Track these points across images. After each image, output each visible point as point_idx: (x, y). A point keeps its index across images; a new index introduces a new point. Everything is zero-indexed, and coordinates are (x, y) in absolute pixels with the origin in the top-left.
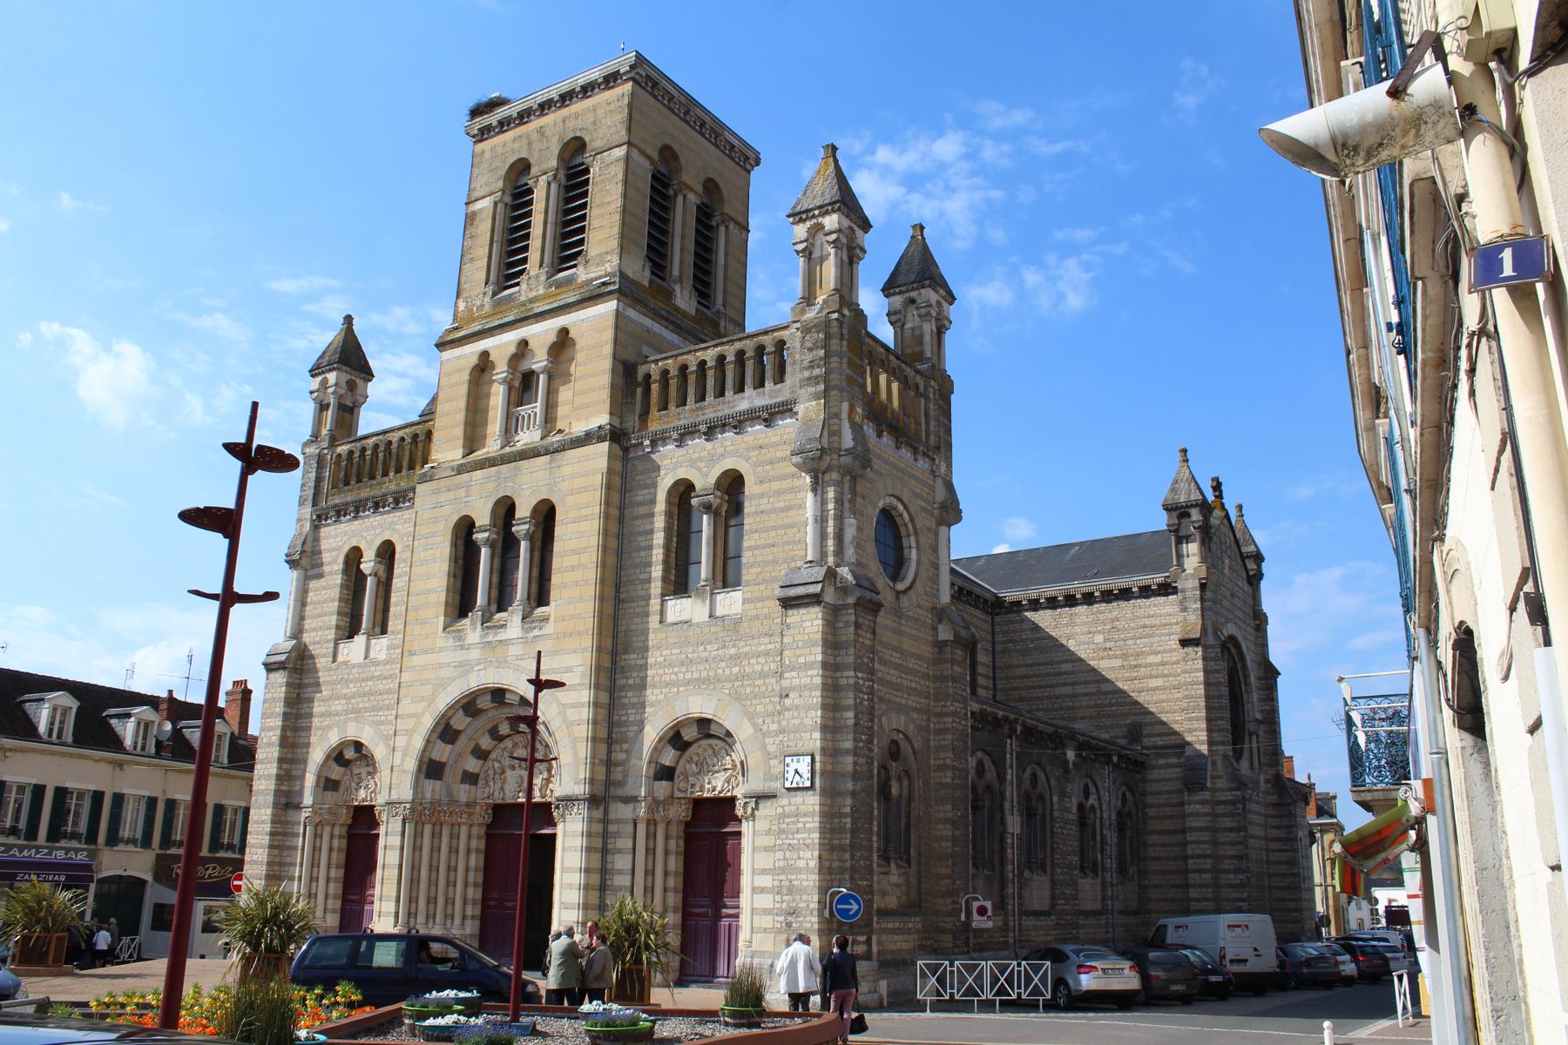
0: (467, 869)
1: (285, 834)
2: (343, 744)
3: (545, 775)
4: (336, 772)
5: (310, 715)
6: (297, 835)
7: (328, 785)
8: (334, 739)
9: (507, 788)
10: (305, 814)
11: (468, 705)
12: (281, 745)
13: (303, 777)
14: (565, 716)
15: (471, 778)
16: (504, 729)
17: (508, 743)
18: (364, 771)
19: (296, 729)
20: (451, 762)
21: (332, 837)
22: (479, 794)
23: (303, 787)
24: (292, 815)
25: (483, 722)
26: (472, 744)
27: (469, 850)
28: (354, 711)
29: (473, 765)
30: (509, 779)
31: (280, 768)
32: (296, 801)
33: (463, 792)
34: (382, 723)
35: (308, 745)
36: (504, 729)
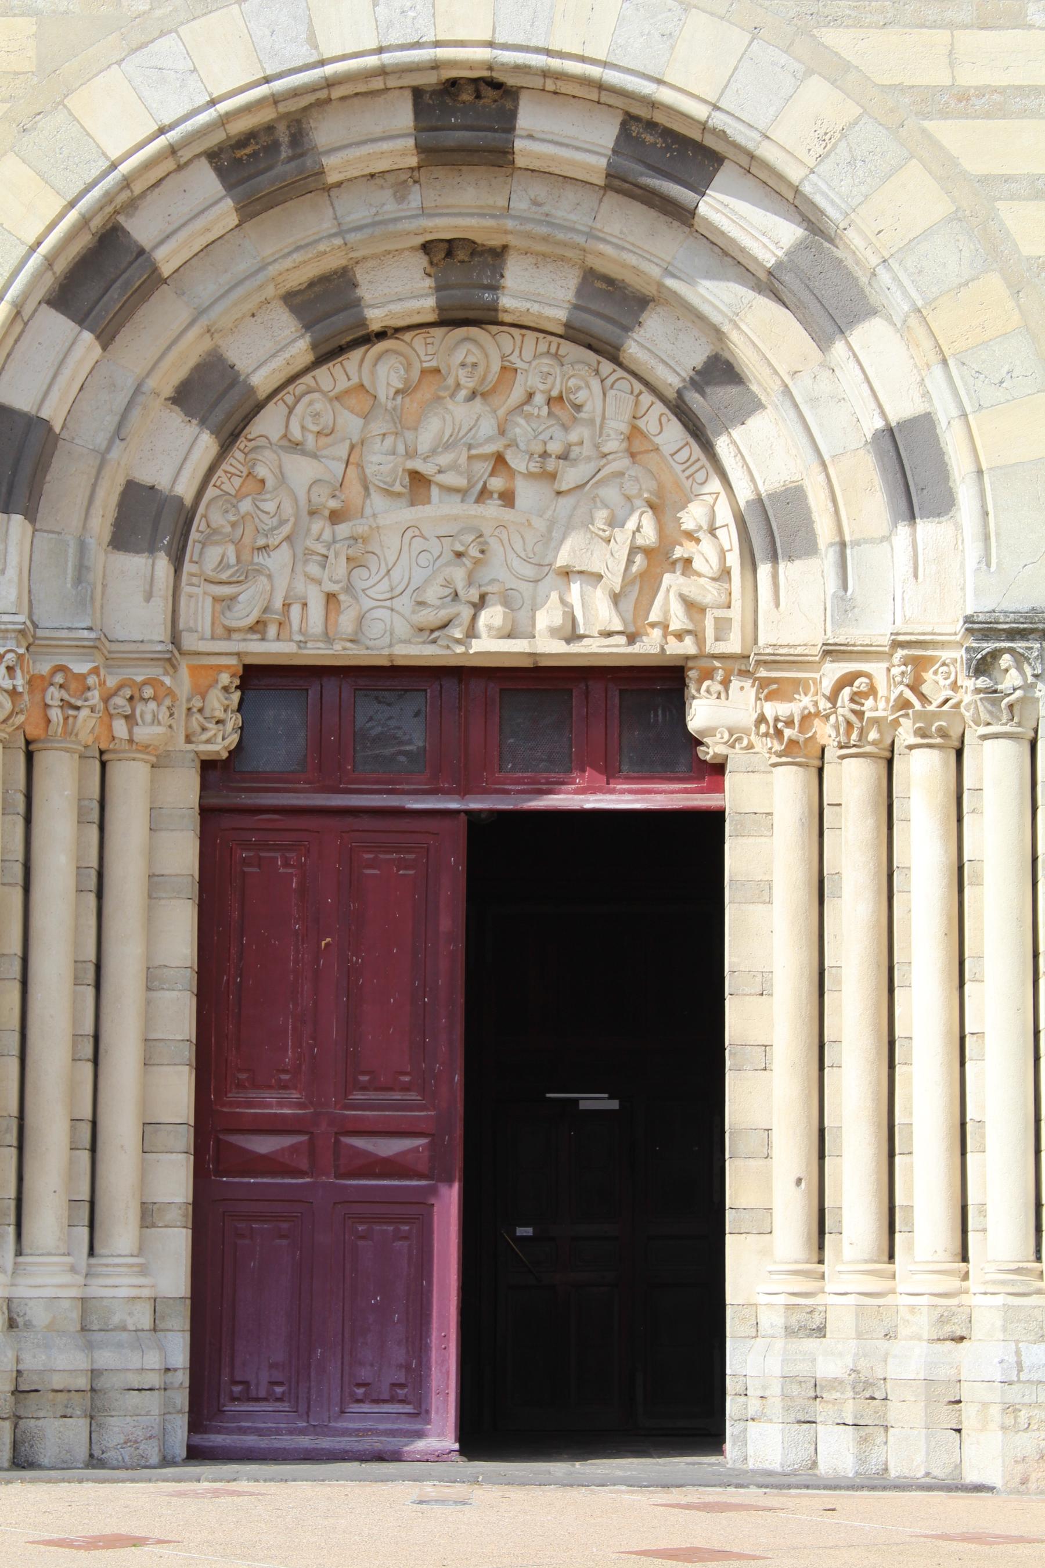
0: (153, 980)
3: (649, 535)
9: (373, 584)
11: (261, 157)
14: (993, 249)
15: (152, 521)
16: (397, 292)
17: (383, 371)
20: (92, 431)
22: (199, 612)
25: (299, 244)
26: (207, 344)
27: (154, 882)
29: (175, 455)
30: (390, 544)
33: (135, 594)
36: (397, 292)
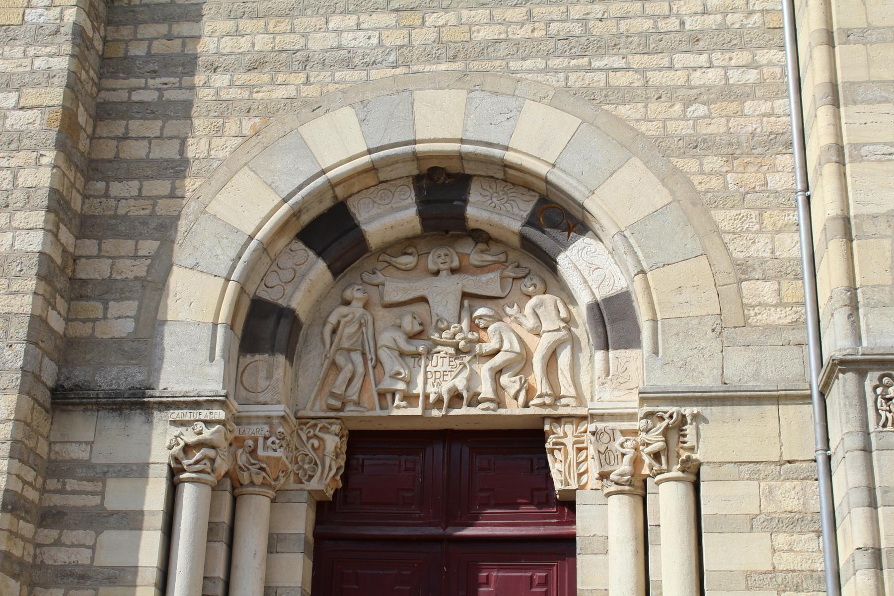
1: (49, 517)
2: (373, 176)
4: (307, 282)
5: (187, 64)
6: (132, 520)
7: (262, 327)
8: (338, 144)
10: (163, 440)
12: (60, 146)
13: (154, 285)
18: (444, 293)
19: (103, 112)
21: (274, 543)
23: (151, 326)
24: (93, 438)
28: (442, 50)
31: (53, 233)
32: (114, 377)
34: (624, 96)
35: (178, 168)
